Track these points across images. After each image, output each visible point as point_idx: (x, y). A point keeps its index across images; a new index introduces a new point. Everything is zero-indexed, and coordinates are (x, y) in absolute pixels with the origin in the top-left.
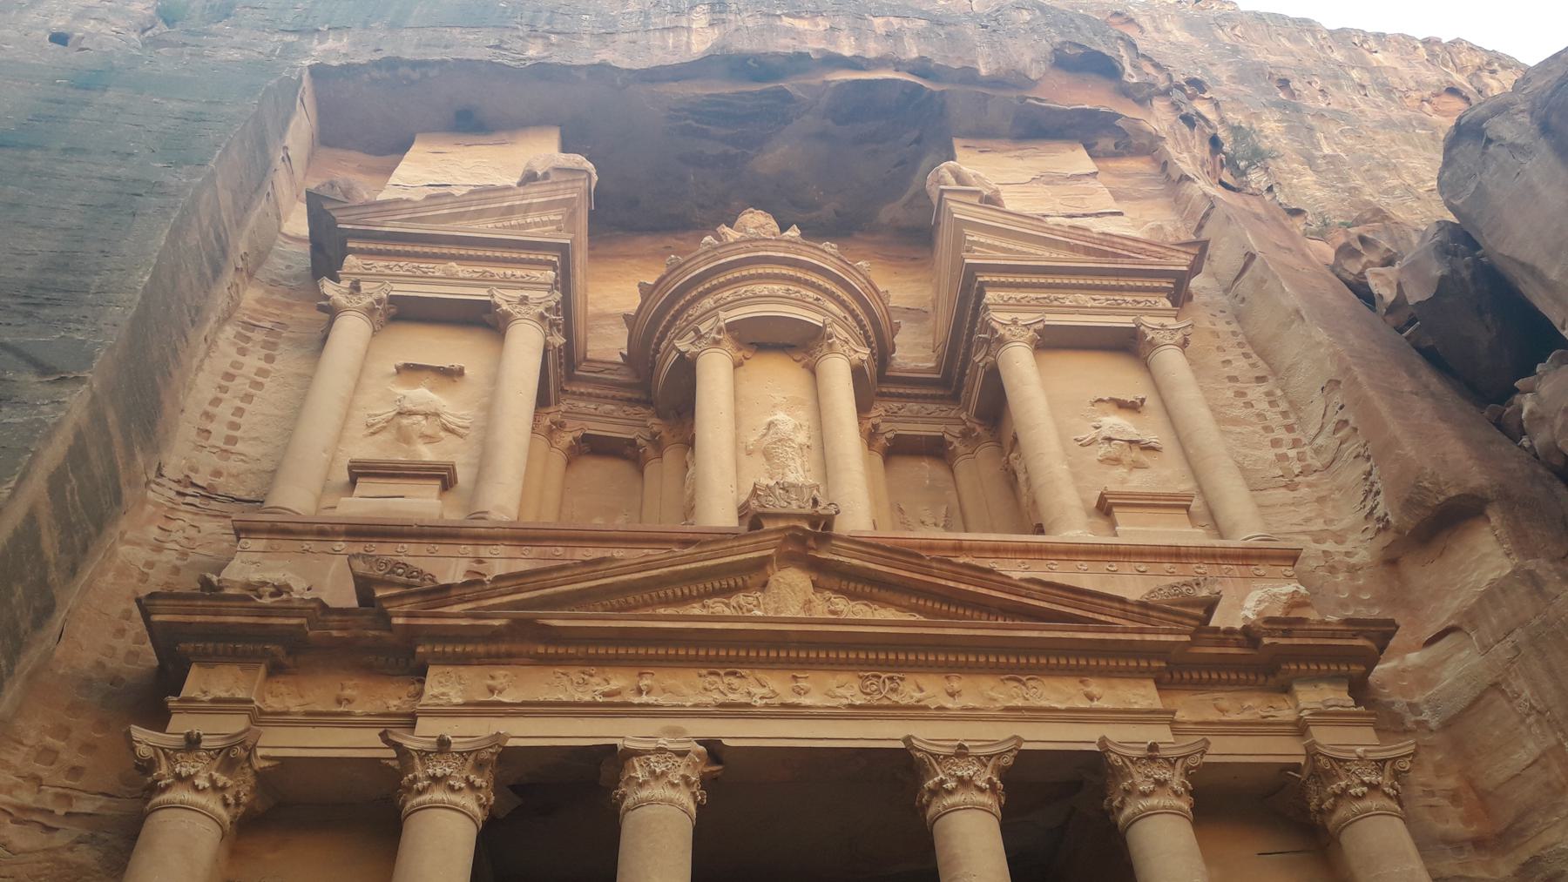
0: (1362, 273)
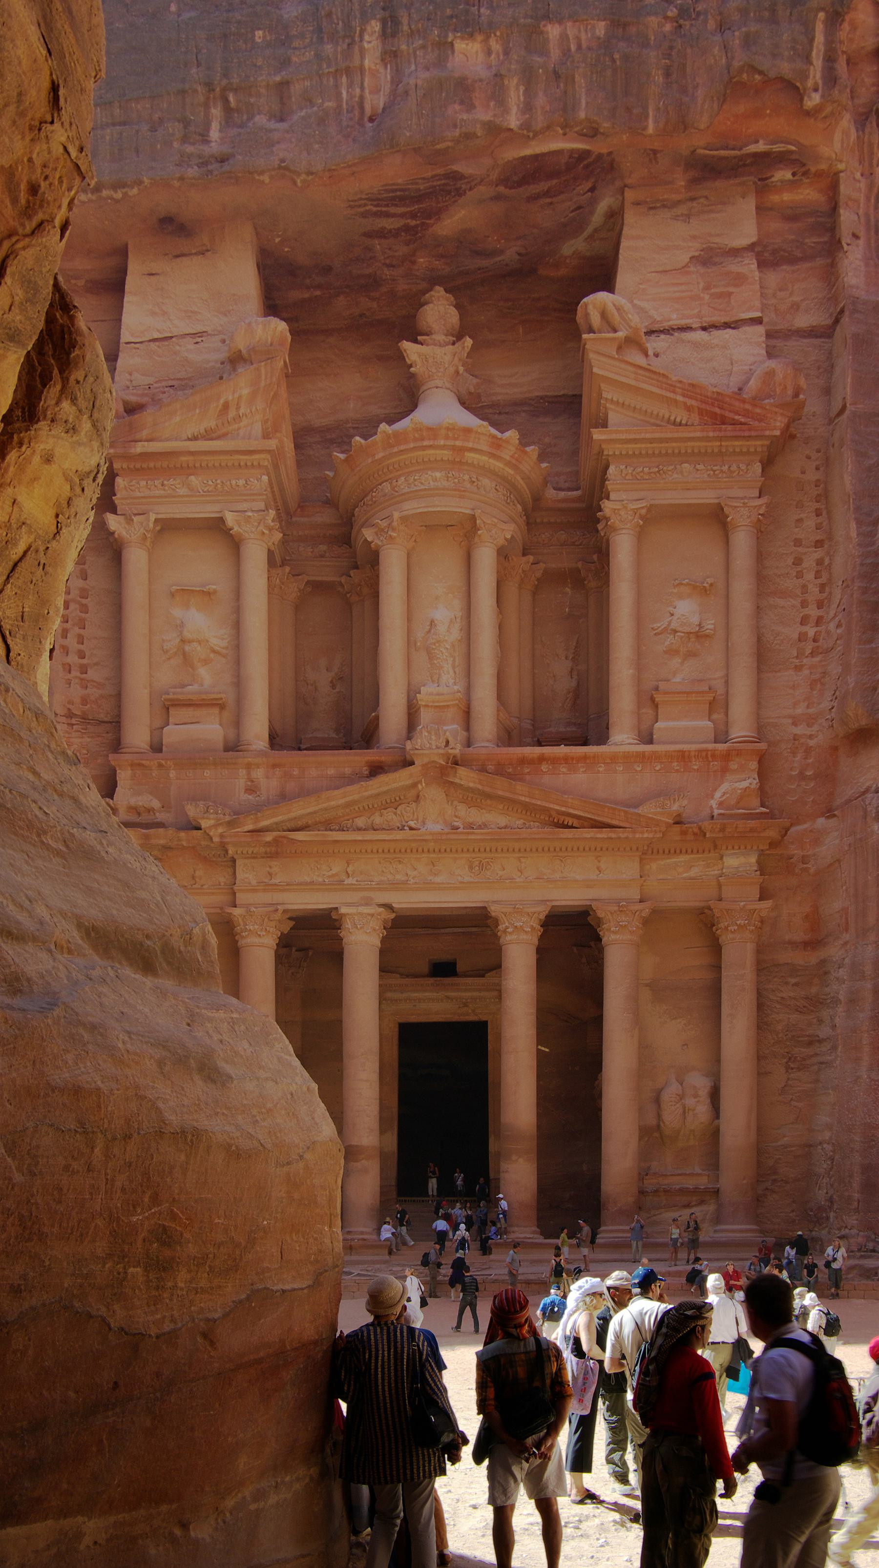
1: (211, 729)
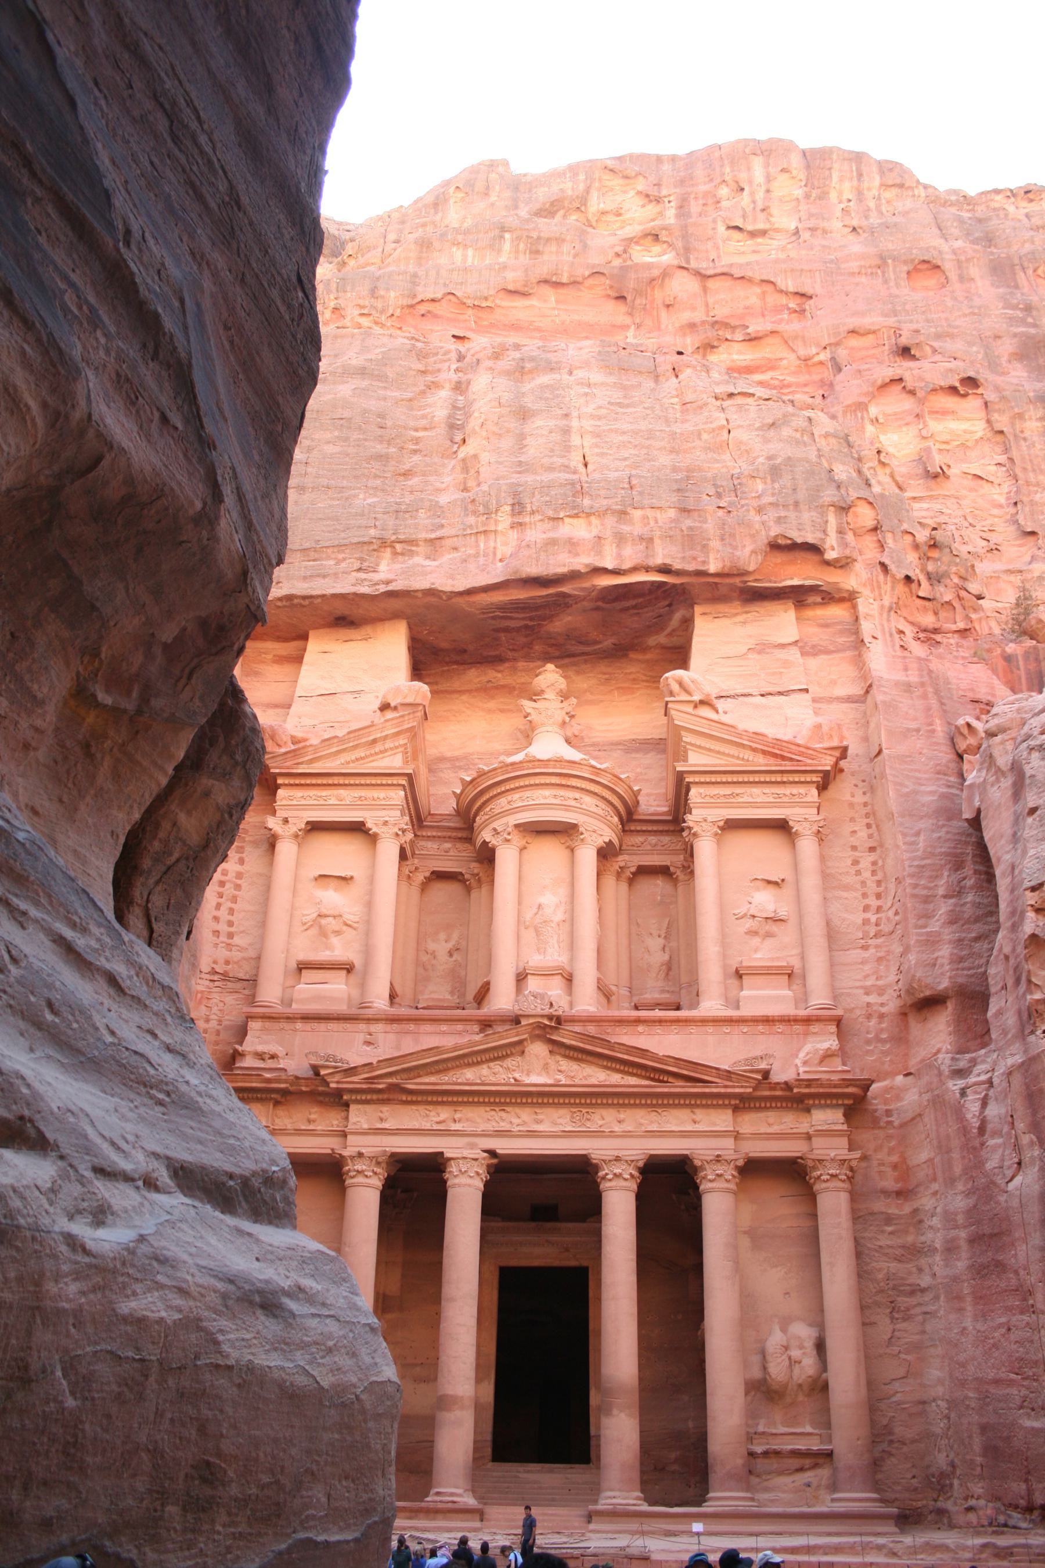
0: (965, 752)
1: (335, 991)
